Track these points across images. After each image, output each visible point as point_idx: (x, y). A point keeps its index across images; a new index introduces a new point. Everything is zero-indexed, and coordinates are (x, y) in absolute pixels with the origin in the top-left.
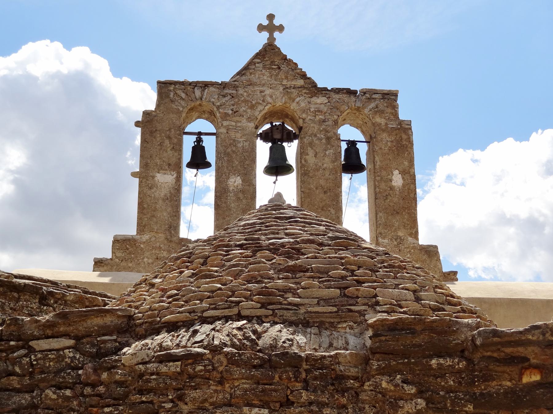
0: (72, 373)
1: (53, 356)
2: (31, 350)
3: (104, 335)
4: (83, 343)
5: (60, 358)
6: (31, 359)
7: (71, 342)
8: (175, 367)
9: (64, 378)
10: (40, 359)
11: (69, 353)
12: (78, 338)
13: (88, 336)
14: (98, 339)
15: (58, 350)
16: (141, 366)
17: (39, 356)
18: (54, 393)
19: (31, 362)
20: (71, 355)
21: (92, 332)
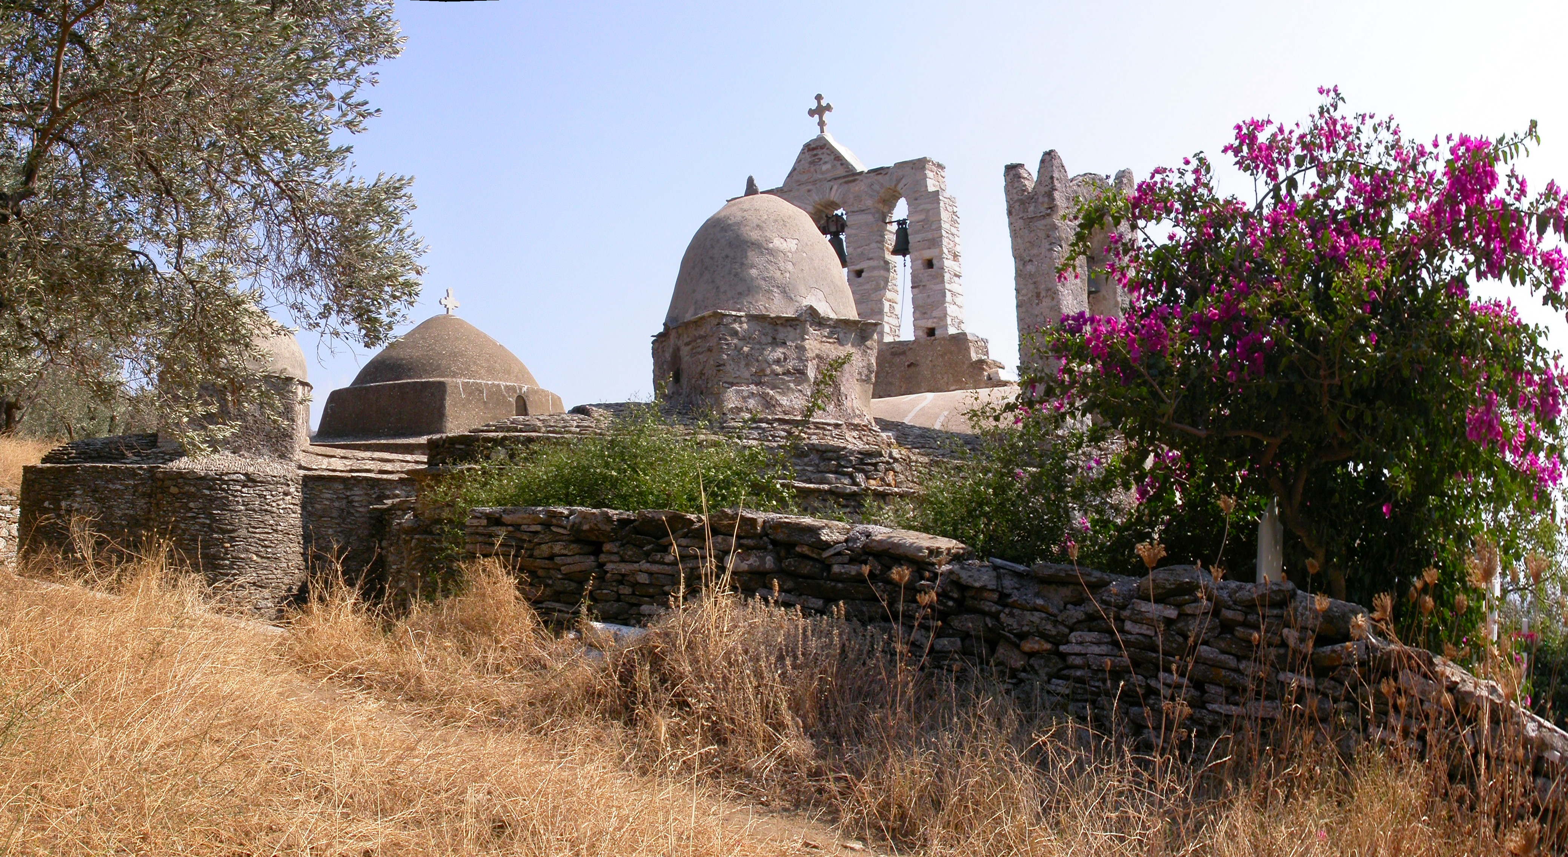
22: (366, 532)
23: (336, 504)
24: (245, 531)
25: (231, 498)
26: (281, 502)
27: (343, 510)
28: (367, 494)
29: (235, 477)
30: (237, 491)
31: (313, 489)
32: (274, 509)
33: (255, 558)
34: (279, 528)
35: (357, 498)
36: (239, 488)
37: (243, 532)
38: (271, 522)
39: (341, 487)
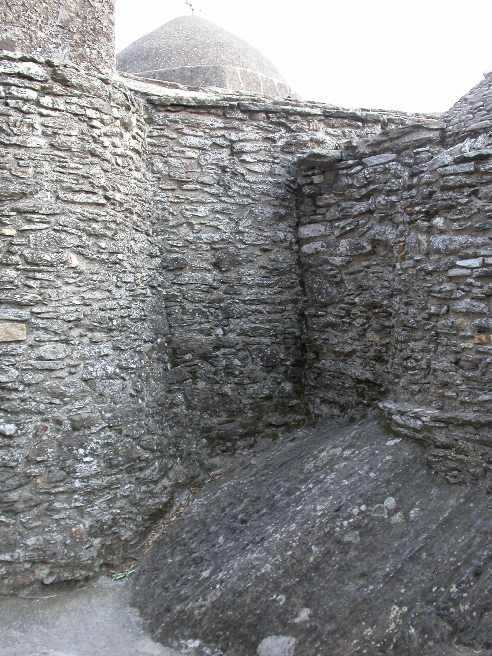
0: (396, 183)
1: (381, 170)
2: (364, 166)
3: (419, 147)
4: (402, 156)
5: (386, 171)
6: (364, 173)
7: (393, 156)
8: (469, 167)
9: (389, 186)
10: (372, 173)
11: (393, 165)
12: (398, 152)
13: (407, 149)
14: (415, 151)
15: (383, 164)
16: (441, 169)
17: (371, 170)
18: (384, 200)
19: (365, 176)
20: (394, 167)
21: (409, 146)
22: (269, 211)
23: (212, 156)
24: (50, 198)
25: (15, 116)
26: (117, 140)
27: (224, 169)
28: (267, 139)
29: (22, 67)
30: (26, 101)
31: (163, 126)
32: (107, 154)
33: (75, 261)
34: (118, 197)
35: (249, 147)
36: (33, 95)
37: (44, 200)
38: (103, 182)
39: (219, 123)
